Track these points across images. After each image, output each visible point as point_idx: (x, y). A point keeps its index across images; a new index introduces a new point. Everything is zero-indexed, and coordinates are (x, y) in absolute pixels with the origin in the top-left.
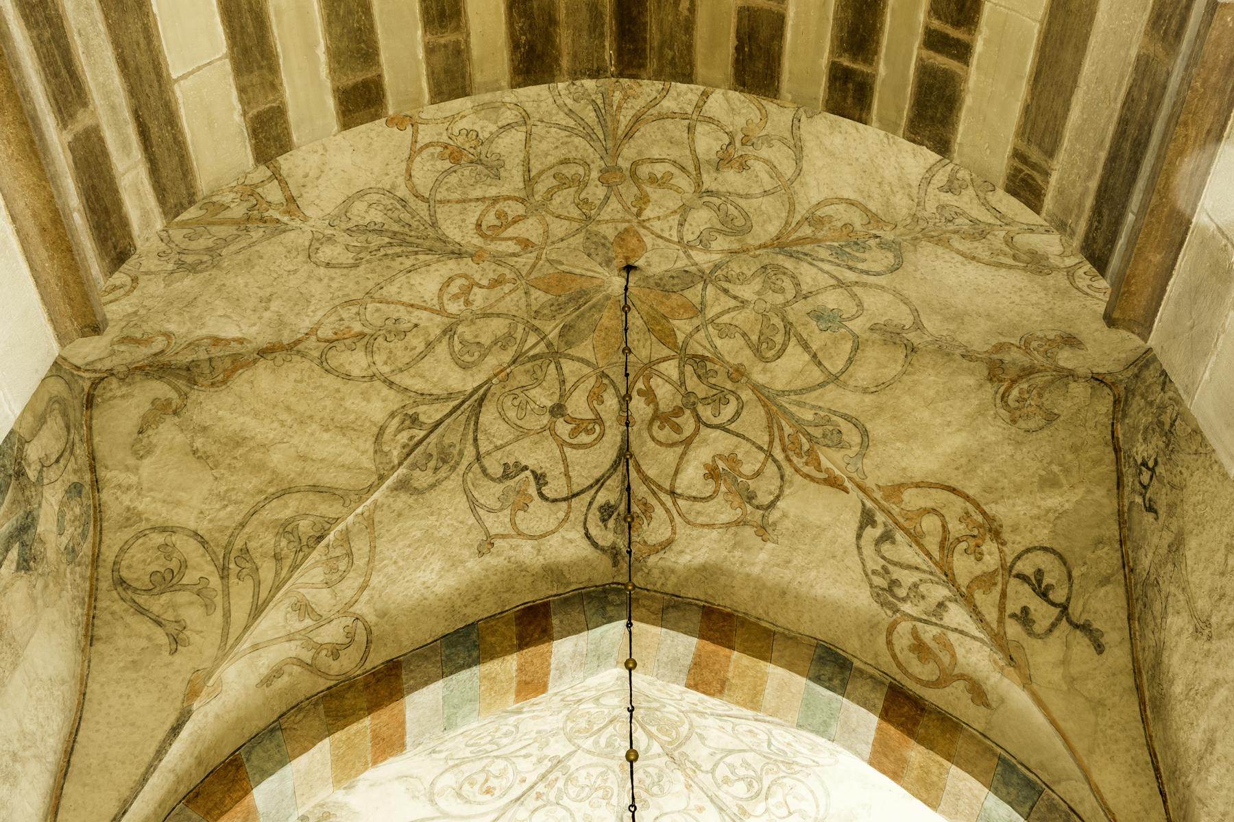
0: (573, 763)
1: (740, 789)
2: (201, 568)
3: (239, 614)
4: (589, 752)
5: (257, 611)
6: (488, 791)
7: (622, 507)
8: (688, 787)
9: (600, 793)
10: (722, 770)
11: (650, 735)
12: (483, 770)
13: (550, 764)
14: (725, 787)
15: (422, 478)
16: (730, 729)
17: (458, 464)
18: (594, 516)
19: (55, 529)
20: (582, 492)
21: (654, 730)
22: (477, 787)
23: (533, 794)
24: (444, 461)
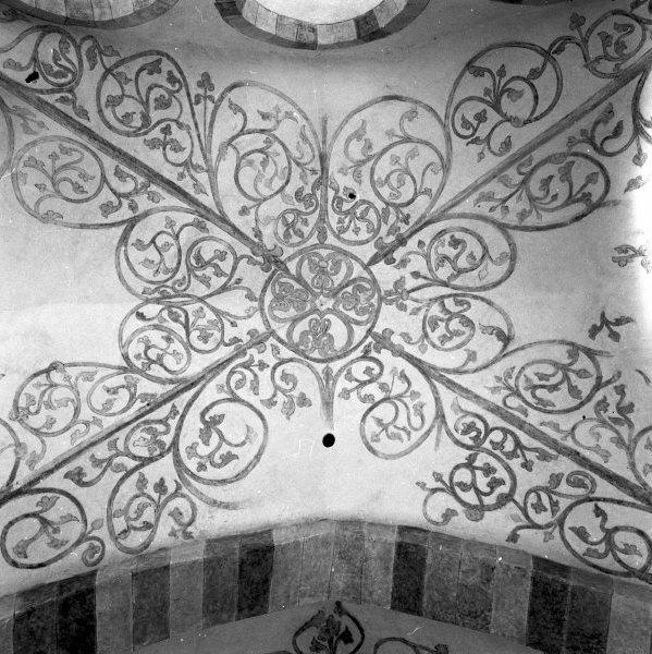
0: (368, 252)
1: (208, 251)
4: (356, 259)
7: (335, 639)
8: (258, 234)
9: (346, 207)
10: (226, 266)
11: (299, 279)
12: (460, 272)
13: (395, 255)
14: (222, 248)
16: (227, 325)
21: (297, 286)
22: (467, 251)
23: (412, 221)
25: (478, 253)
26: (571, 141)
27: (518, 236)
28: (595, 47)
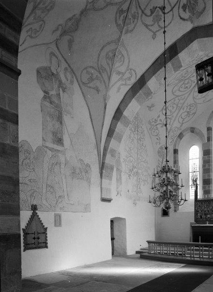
2: (95, 74)
3: (107, 81)
5: (109, 78)
6: (187, 87)
15: (131, 27)
17: (138, 17)
18: (181, 10)
19: (65, 80)
20: (175, 5)
24: (134, 18)
25: (181, 89)
26: (173, 117)
27: (174, 97)
28: (176, 129)
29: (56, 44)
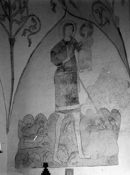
29: (69, 13)
